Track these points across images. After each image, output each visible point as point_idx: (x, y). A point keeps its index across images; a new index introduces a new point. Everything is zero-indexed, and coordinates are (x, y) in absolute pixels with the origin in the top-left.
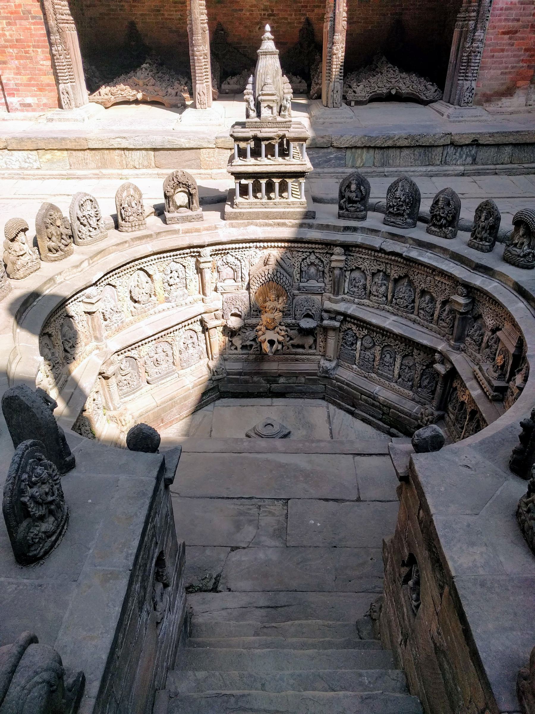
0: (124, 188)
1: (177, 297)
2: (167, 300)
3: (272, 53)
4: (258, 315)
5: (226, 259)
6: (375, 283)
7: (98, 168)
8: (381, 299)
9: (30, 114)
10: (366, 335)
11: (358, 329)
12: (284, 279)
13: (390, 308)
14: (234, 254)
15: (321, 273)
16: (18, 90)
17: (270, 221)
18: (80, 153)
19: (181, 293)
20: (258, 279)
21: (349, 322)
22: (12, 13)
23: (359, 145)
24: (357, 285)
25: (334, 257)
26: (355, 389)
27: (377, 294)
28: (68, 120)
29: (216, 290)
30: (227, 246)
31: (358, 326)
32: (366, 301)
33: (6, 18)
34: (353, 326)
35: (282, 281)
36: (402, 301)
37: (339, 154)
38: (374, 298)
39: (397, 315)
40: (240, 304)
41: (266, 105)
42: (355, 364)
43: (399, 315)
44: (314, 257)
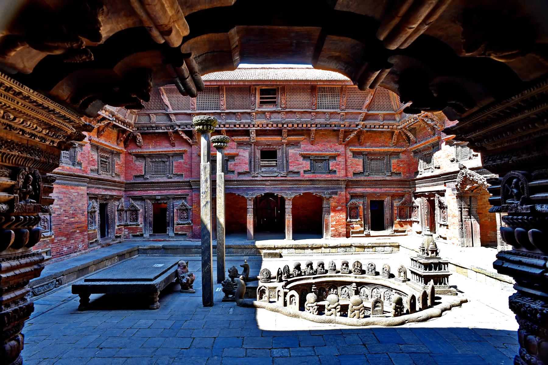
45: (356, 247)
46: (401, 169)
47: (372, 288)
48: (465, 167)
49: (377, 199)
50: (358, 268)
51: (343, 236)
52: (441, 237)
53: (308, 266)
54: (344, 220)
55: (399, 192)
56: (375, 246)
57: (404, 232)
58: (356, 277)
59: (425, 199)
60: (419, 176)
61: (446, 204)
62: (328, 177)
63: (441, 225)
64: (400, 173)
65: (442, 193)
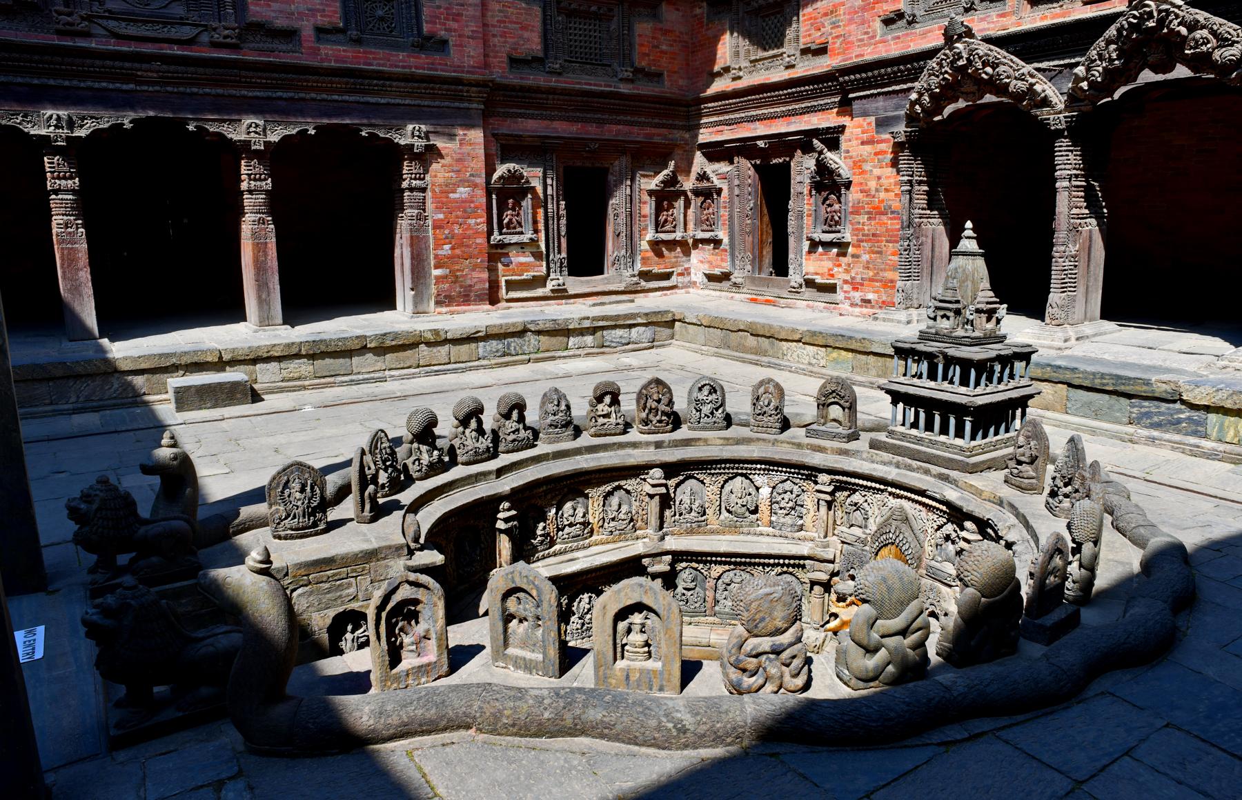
0: (761, 383)
2: (771, 524)
3: (964, 254)
7: (879, 376)
9: (865, 310)
16: (862, 285)
17: (915, 464)
18: (863, 357)
19: (790, 522)
22: (874, 208)
23: (1228, 406)
25: (964, 534)
28: (892, 321)
30: (853, 480)
33: (868, 213)
37: (1195, 415)
41: (942, 313)
45: (539, 333)
46: (664, 61)
47: (721, 479)
48: (969, 33)
49: (588, 164)
50: (662, 407)
51: (480, 299)
52: (810, 283)
53: (464, 422)
54: (481, 240)
55: (657, 139)
56: (603, 328)
57: (667, 276)
58: (658, 445)
59: (745, 166)
60: (718, 86)
61: (845, 171)
62: (418, 63)
63: (814, 245)
64: (660, 75)
65: (832, 138)
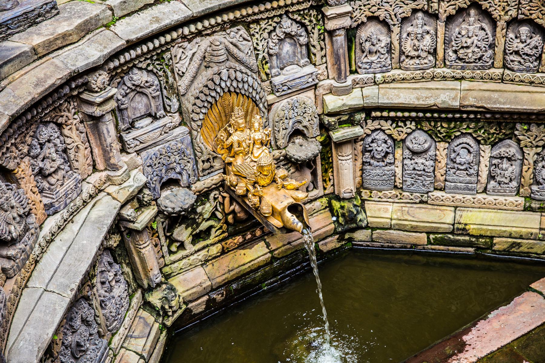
1: (66, 195)
2: (51, 210)
4: (212, 167)
5: (131, 79)
6: (408, 35)
8: (426, 61)
10: (414, 131)
11: (394, 125)
12: (250, 78)
13: (445, 69)
14: (143, 65)
15: (304, 47)
20: (204, 98)
21: (375, 119)
24: (374, 49)
26: (414, 229)
27: (416, 53)
29: (123, 150)
31: (394, 120)
32: (396, 73)
34: (382, 122)
35: (246, 86)
36: (470, 51)
38: (412, 62)
39: (463, 78)
40: (177, 158)
42: (396, 187)
43: (468, 76)
44: (289, 21)
